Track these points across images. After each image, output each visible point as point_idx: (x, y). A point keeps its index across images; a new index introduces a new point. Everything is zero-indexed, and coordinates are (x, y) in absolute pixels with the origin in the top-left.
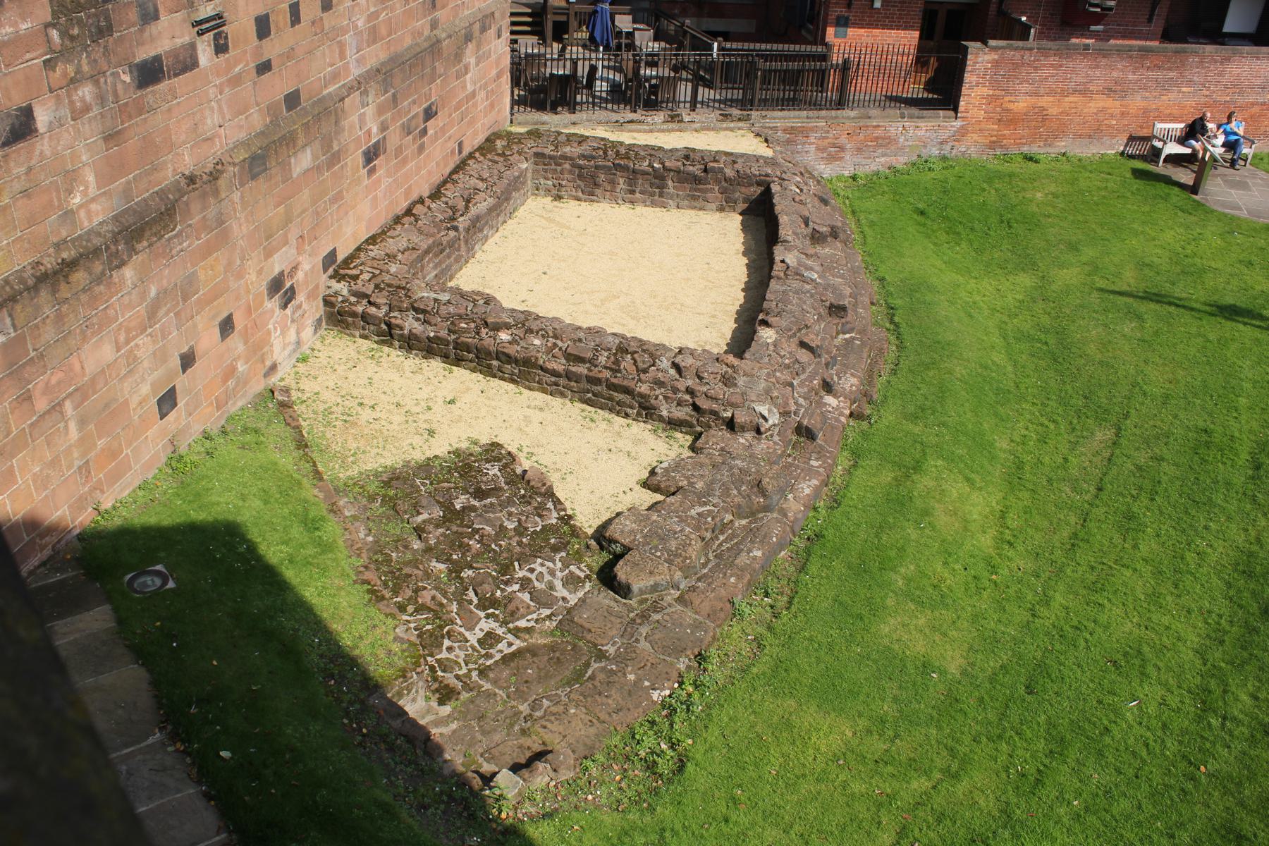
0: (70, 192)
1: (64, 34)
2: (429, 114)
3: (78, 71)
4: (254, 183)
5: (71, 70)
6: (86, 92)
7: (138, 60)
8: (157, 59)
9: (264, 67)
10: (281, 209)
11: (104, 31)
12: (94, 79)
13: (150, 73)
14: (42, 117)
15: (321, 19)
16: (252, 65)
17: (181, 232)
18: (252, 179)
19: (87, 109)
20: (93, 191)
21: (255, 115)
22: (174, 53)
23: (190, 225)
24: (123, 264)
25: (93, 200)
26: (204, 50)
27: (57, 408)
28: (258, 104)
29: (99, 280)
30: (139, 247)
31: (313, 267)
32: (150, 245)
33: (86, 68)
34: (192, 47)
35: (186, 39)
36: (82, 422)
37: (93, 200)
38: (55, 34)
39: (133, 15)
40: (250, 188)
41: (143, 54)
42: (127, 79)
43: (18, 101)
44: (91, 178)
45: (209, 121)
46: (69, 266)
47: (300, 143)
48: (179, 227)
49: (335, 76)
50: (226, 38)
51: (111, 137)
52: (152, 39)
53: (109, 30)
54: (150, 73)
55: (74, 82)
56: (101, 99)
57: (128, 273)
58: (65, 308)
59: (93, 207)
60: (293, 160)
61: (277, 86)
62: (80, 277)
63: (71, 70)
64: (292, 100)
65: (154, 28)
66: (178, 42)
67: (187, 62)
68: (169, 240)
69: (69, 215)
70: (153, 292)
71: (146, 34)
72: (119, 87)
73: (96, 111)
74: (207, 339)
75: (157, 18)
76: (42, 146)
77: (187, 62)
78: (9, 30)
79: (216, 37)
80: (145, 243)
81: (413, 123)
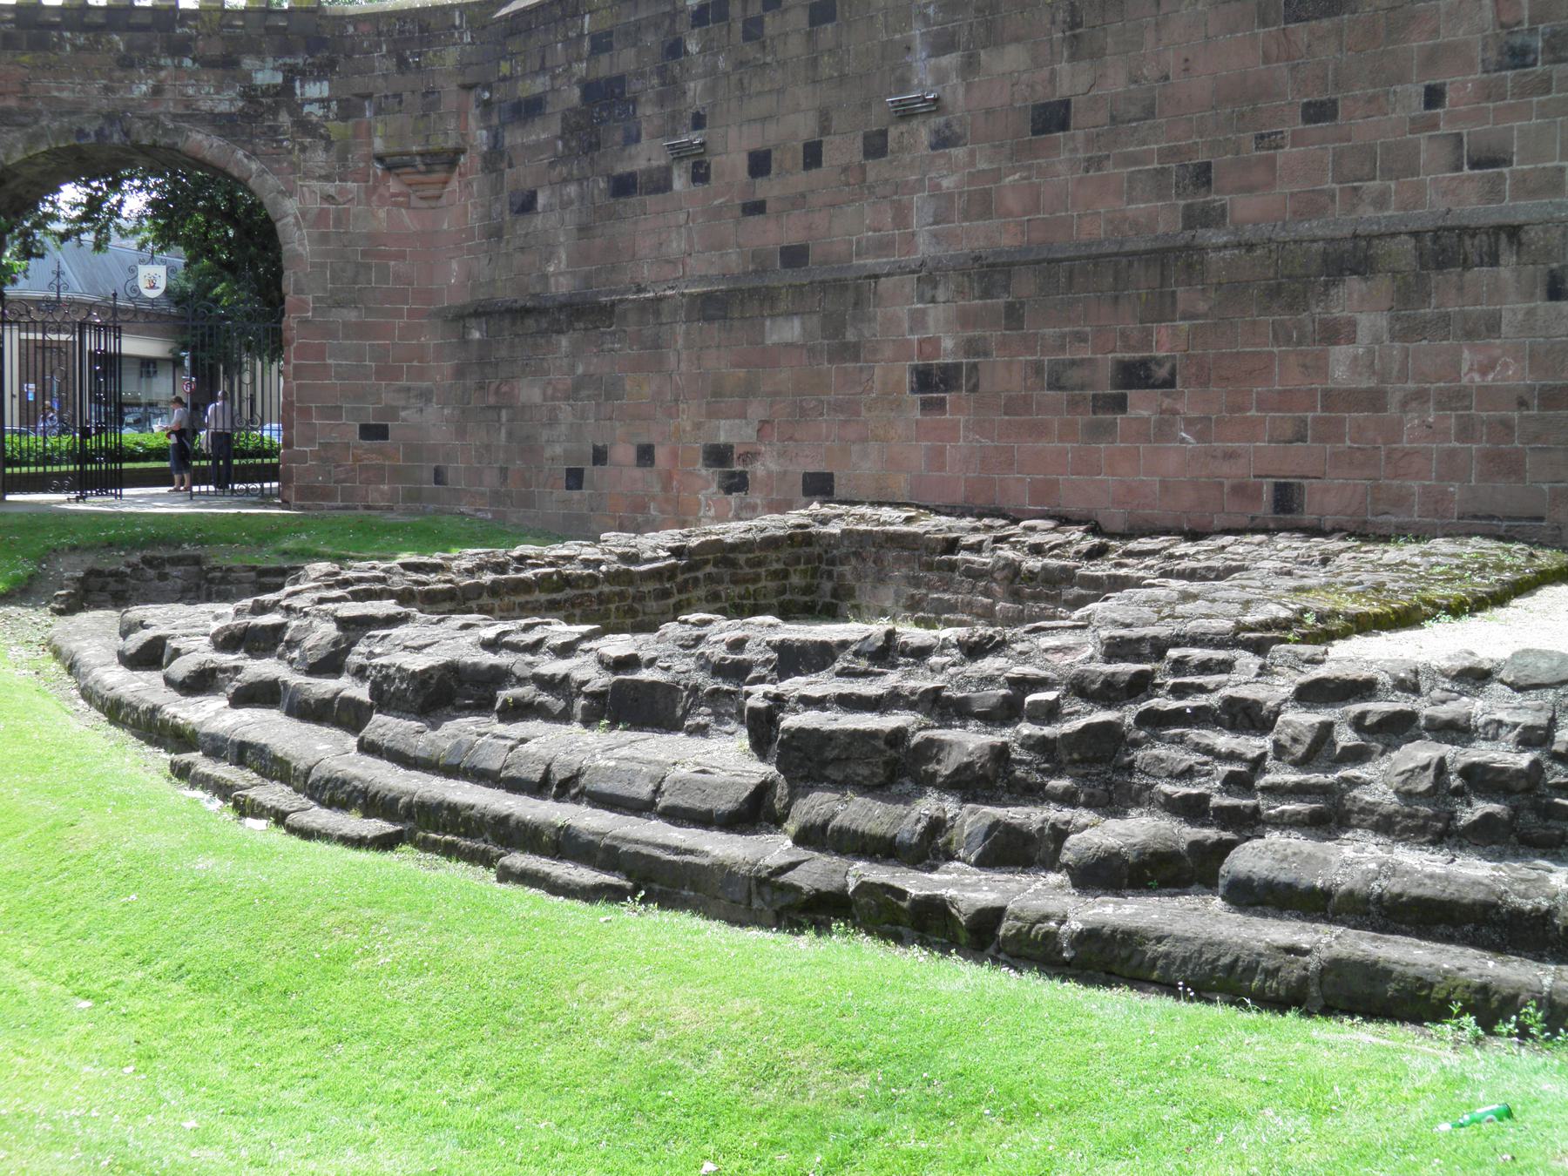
0: (548, 261)
1: (565, 145)
2: (1135, 375)
3: (570, 173)
4: (706, 325)
5: (565, 171)
6: (572, 190)
7: (615, 174)
8: (632, 175)
9: (755, 208)
10: (742, 372)
11: (594, 146)
12: (580, 181)
13: (624, 186)
14: (542, 200)
15: (863, 168)
16: (738, 202)
17: (613, 333)
18: (705, 320)
19: (571, 202)
20: (563, 266)
21: (734, 257)
22: (649, 172)
23: (625, 331)
24: (560, 332)
25: (561, 274)
26: (679, 176)
27: (497, 408)
28: (739, 246)
29: (542, 333)
30: (576, 325)
31: (785, 473)
32: (586, 329)
33: (575, 172)
34: (668, 170)
35: (663, 162)
36: (510, 434)
37: (561, 274)
38: (560, 144)
39: (618, 136)
40: (701, 328)
41: (621, 169)
42: (602, 185)
43: (528, 184)
44: (564, 257)
45: (675, 245)
46: (526, 312)
47: (782, 306)
48: (613, 328)
49: (884, 246)
50: (708, 168)
51: (584, 230)
52: (631, 157)
53: (598, 145)
54: (624, 186)
55: (565, 181)
56: (582, 198)
57: (564, 342)
58: (517, 340)
59: (561, 279)
60: (768, 323)
61: (772, 234)
62: (530, 323)
63: (565, 171)
64: (794, 256)
65: (633, 149)
66: (654, 163)
67: (661, 184)
68: (604, 333)
69: (544, 277)
70: (580, 370)
71: (627, 152)
72: (596, 192)
73: (575, 207)
74: (623, 453)
75: (637, 140)
76: (538, 221)
77: (661, 184)
78: (534, 137)
79: (696, 165)
80: (582, 325)
81: (1075, 375)
